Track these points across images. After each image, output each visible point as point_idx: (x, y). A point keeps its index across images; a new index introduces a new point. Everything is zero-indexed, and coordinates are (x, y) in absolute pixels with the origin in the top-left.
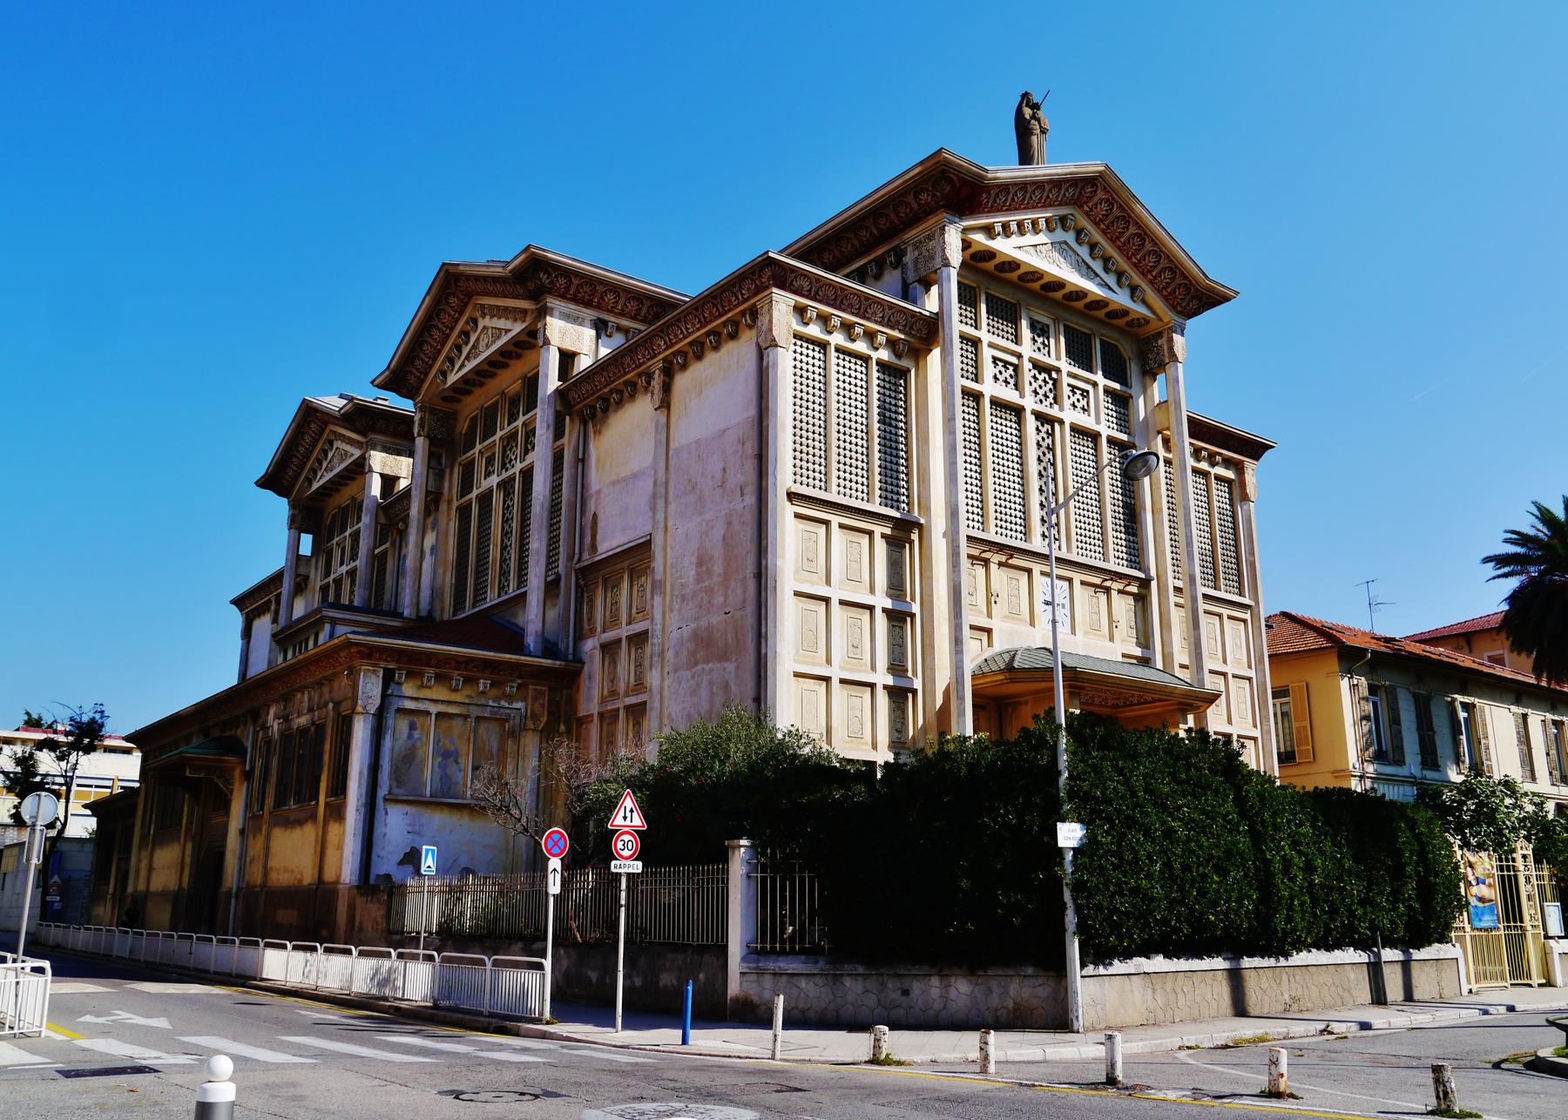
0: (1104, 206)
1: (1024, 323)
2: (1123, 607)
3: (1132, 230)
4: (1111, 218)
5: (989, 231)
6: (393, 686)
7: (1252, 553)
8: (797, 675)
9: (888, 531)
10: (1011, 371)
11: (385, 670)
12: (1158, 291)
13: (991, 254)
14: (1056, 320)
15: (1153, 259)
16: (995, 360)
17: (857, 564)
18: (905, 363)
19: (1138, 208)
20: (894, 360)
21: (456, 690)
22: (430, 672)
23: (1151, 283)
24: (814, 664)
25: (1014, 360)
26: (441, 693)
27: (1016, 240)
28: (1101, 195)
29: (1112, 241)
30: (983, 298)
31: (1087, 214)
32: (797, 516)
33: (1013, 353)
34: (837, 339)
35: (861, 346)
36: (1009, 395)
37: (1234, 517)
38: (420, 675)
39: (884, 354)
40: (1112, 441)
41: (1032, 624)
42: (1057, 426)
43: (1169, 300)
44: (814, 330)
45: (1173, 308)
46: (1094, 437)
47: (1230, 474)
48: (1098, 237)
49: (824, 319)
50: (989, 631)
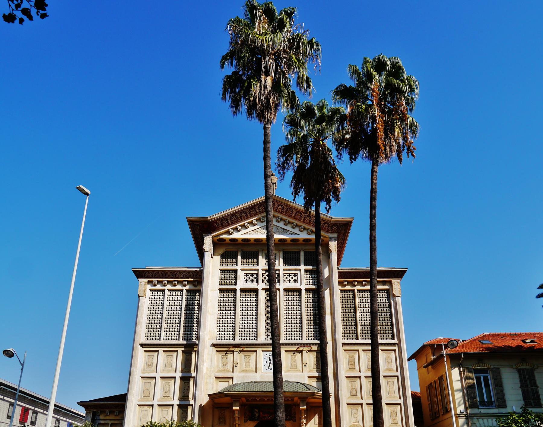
1: (260, 257)
2: (310, 358)
3: (295, 211)
5: (228, 233)
6: (97, 417)
7: (397, 319)
8: (139, 405)
9: (183, 349)
10: (255, 276)
11: (93, 412)
13: (234, 240)
14: (279, 251)
16: (246, 275)
18: (198, 288)
21: (116, 415)
22: (107, 411)
24: (149, 401)
25: (256, 272)
26: (112, 417)
27: (243, 231)
29: (291, 216)
30: (240, 254)
32: (145, 351)
33: (255, 270)
34: (169, 287)
35: (179, 287)
36: (253, 286)
38: (104, 412)
39: (187, 287)
40: (307, 290)
41: (256, 372)
44: (159, 287)
46: (299, 291)
47: (386, 287)
48: (284, 217)
50: (232, 378)
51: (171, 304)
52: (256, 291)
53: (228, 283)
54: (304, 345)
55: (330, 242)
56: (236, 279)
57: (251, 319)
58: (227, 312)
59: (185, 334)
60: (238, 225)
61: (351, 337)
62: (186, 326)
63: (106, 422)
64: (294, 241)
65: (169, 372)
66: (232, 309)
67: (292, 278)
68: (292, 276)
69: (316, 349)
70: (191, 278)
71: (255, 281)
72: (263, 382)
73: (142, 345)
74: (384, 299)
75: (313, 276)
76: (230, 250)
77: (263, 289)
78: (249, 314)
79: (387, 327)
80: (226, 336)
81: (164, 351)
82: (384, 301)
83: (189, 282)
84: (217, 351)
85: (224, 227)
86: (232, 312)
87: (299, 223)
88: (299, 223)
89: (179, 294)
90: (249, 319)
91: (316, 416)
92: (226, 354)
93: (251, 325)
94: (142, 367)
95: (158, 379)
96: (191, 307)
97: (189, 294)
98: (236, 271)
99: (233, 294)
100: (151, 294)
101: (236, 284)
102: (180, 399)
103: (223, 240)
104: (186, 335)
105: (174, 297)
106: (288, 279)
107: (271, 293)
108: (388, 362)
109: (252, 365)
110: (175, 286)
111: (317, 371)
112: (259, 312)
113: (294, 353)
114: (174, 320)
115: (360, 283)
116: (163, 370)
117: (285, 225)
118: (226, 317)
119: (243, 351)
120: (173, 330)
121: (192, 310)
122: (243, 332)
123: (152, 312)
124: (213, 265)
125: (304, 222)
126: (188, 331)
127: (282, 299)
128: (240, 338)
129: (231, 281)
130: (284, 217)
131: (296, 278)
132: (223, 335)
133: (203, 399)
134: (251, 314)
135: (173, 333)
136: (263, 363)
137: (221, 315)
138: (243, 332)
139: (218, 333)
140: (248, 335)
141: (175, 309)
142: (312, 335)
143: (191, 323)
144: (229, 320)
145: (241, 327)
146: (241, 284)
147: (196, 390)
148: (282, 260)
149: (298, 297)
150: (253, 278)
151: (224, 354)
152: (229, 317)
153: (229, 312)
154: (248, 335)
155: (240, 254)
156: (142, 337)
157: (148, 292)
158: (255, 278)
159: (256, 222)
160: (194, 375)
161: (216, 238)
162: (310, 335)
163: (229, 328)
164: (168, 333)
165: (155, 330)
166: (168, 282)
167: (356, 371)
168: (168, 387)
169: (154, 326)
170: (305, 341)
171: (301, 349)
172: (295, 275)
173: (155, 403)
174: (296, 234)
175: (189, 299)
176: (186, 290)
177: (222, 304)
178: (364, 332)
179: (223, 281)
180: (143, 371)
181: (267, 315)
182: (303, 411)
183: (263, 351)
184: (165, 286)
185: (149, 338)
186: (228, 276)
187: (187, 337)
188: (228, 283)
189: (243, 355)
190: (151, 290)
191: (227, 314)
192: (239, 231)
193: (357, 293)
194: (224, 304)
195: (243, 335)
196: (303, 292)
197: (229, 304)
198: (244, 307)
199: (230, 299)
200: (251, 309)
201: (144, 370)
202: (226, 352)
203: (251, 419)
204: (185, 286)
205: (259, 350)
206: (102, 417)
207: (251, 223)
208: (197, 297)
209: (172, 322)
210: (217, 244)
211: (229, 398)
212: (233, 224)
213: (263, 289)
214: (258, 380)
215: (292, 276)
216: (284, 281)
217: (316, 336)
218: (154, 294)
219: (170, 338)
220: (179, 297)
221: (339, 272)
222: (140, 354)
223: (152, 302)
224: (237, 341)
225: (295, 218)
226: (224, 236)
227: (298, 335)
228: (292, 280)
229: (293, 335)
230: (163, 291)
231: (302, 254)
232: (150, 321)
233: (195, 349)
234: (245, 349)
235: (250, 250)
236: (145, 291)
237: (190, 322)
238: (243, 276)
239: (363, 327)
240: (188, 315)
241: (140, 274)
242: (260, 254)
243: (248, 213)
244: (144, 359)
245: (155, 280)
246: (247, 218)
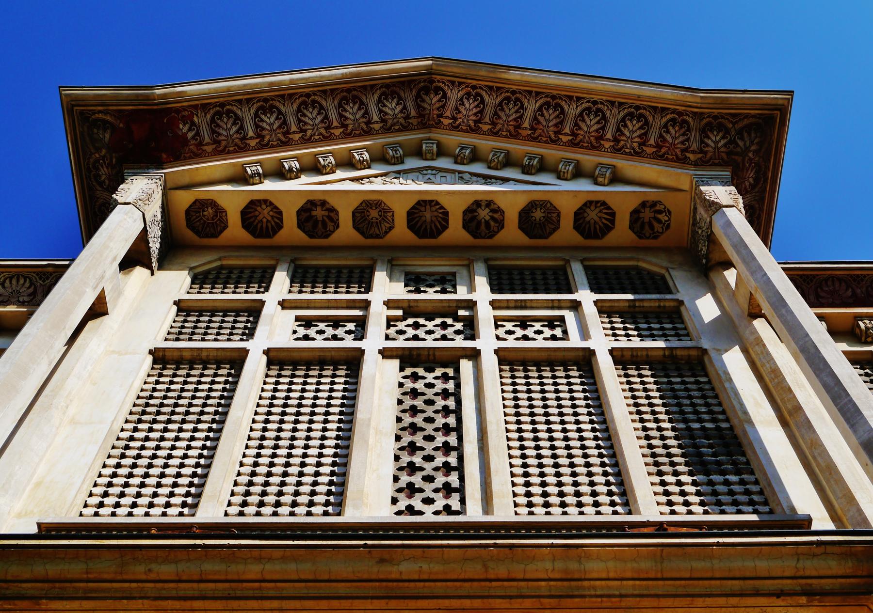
0: (470, 105)
3: (531, 106)
4: (489, 112)
12: (637, 154)
19: (514, 75)
23: (617, 150)
28: (454, 95)
31: (455, 128)
42: (466, 366)
43: (660, 156)
45: (681, 161)
77: (385, 353)
196: (605, 364)
243: (333, 115)
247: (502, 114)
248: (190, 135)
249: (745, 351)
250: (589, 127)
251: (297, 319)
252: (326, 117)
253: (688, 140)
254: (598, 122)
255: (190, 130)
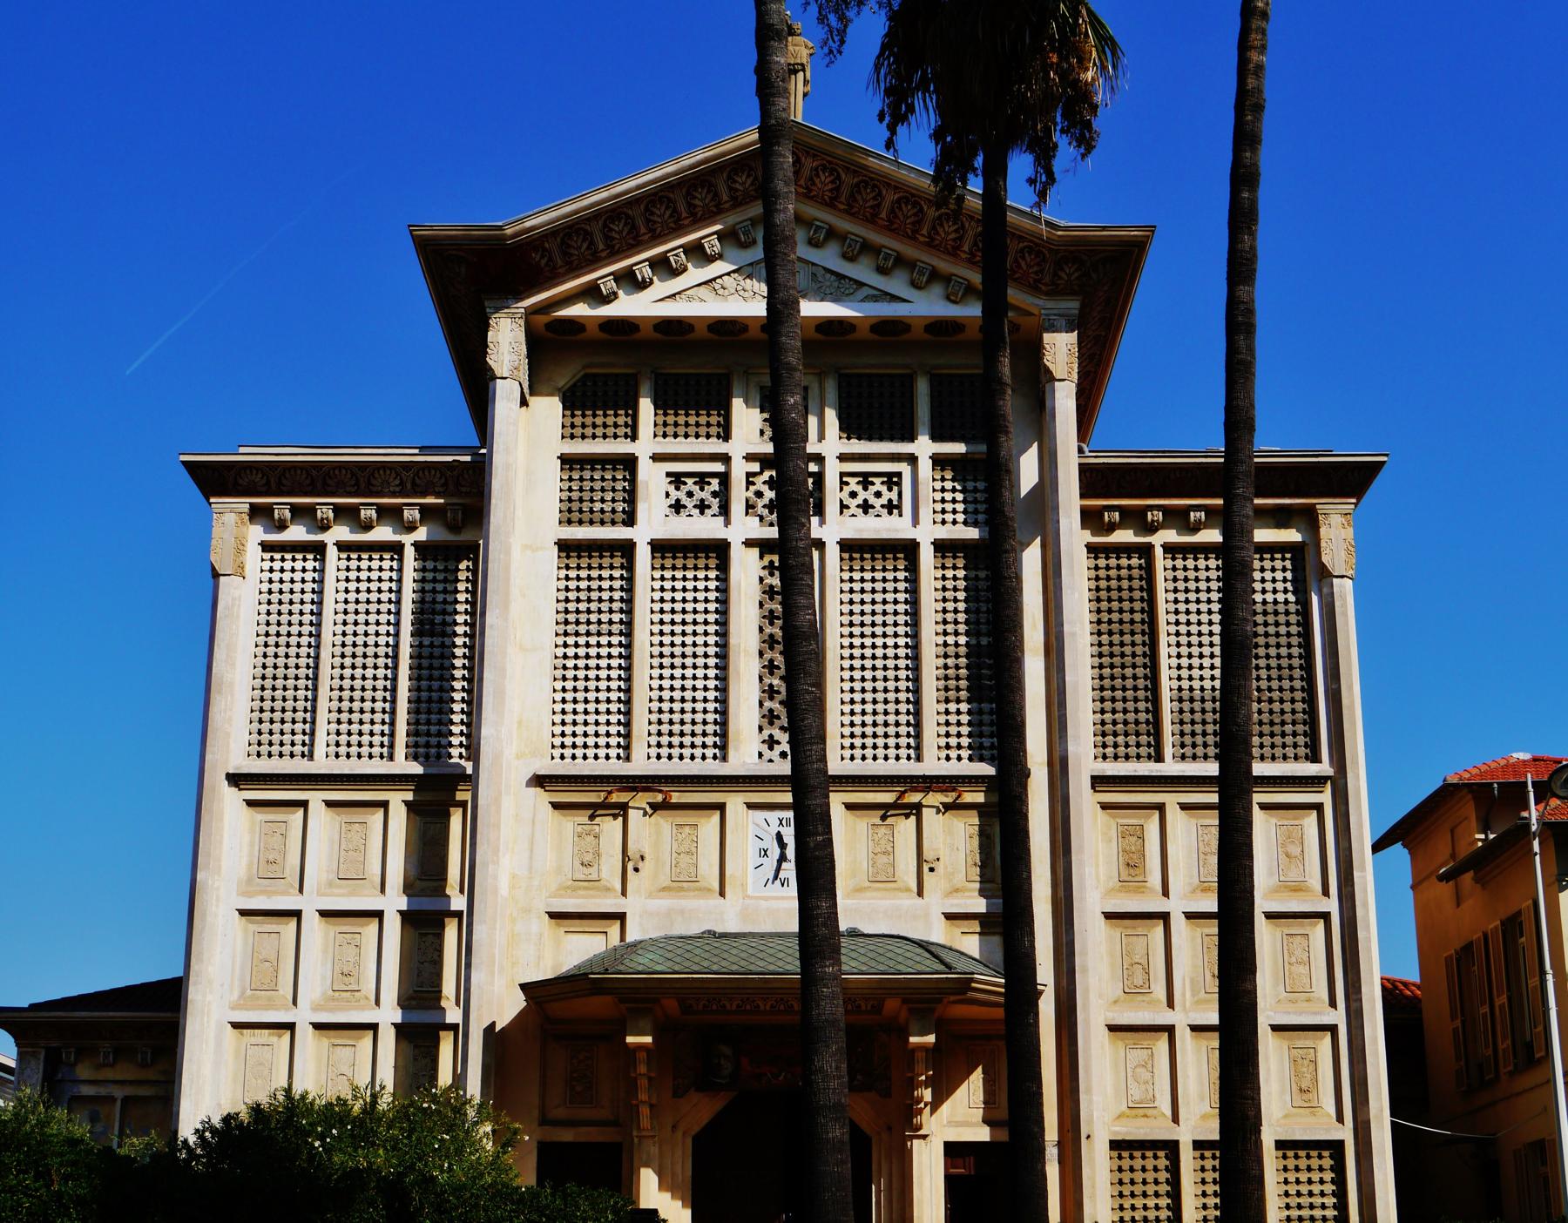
1: (738, 404)
2: (954, 839)
5: (593, 294)
8: (236, 1026)
9: (409, 796)
10: (715, 484)
11: (48, 1050)
15: (950, 227)
16: (677, 479)
17: (358, 856)
20: (451, 537)
25: (718, 467)
27: (661, 288)
29: (871, 220)
30: (645, 387)
32: (251, 803)
34: (342, 532)
35: (383, 533)
37: (1305, 613)
39: (421, 534)
40: (941, 547)
41: (722, 894)
46: (909, 549)
47: (1292, 535)
48: (843, 224)
49: (299, 513)
50: (621, 917)
51: (351, 607)
52: (718, 551)
53: (597, 517)
54: (929, 783)
55: (1047, 337)
56: (631, 497)
57: (700, 673)
58: (593, 640)
59: (417, 734)
60: (638, 261)
61: (1132, 751)
62: (418, 701)
63: (103, 1091)
64: (888, 329)
65: (352, 894)
66: (616, 628)
67: (878, 495)
68: (878, 484)
69: (979, 798)
70: (438, 496)
71: (715, 509)
72: (753, 935)
73: (237, 780)
74: (1280, 586)
75: (970, 485)
76: (600, 373)
77: (749, 543)
78: (689, 650)
79: (1287, 707)
80: (591, 741)
81: (330, 804)
82: (1281, 597)
83: (424, 510)
84: (556, 806)
85: (575, 270)
86: (615, 640)
87: (909, 251)
88: (909, 251)
89: (386, 564)
90: (689, 673)
91: (980, 1069)
92: (592, 817)
93: (700, 695)
94: (242, 872)
95: (311, 921)
96: (438, 619)
97: (430, 564)
98: (629, 463)
99: (617, 562)
100: (266, 565)
101: (630, 520)
102: (405, 1002)
103: (575, 324)
104: (422, 740)
105: (364, 575)
106: (859, 500)
107: (790, 558)
108: (1289, 855)
109: (703, 865)
110: (368, 527)
111: (983, 893)
112: (733, 640)
113: (884, 818)
114: (369, 673)
115: (1175, 517)
116: (330, 884)
117: (848, 257)
118: (592, 663)
119: (665, 806)
120: (367, 717)
121: (444, 634)
122: (665, 728)
123: (272, 640)
124: (530, 439)
125: (931, 245)
126: (428, 723)
127: (834, 588)
128: (654, 751)
129: (607, 507)
130: (843, 224)
131: (894, 496)
132: (580, 741)
133: (498, 1002)
134: (700, 650)
135: (366, 728)
136: (753, 858)
137: (571, 652)
138: (665, 728)
139: (558, 730)
140: (687, 740)
141: (372, 629)
142: (965, 741)
143: (441, 689)
144: (603, 674)
145: (655, 705)
146: (655, 520)
147: (468, 965)
148: (831, 416)
149: (901, 575)
150: (703, 495)
151: (582, 817)
152: (603, 663)
153: (604, 640)
154: (687, 740)
155: (645, 387)
156: (233, 743)
157: (254, 557)
158: (715, 494)
159: (717, 248)
160: (458, 903)
161: (542, 319)
162: (953, 741)
163: (603, 707)
164: (344, 728)
165: (288, 715)
166: (338, 509)
167: (1152, 890)
168: (352, 951)
169: (286, 697)
170: (933, 765)
171: (914, 798)
172: (892, 480)
173: (303, 1016)
174: (894, 298)
175: (428, 587)
176: (416, 545)
177: (572, 606)
178: (1187, 728)
179: (575, 506)
180: (246, 889)
181: (768, 656)
182: (920, 1055)
183: (750, 806)
184: (325, 528)
185: (264, 749)
186: (598, 485)
187: (427, 745)
188: (597, 517)
189: (664, 823)
190: (266, 547)
191: (593, 651)
192: (643, 285)
193: (1160, 561)
194: (583, 606)
195: (665, 740)
196: (927, 555)
197: (605, 606)
198: (667, 618)
199: (606, 584)
200: (700, 629)
201: (249, 881)
202: (594, 810)
203: (705, 1083)
204: (411, 528)
205: (735, 802)
206: (83, 1072)
207: (697, 253)
208: (462, 576)
209: (358, 683)
210: (549, 345)
211: (608, 999)
212: (615, 254)
213: (749, 543)
214: (732, 927)
215: (878, 484)
216: (843, 507)
217: (981, 747)
218: (277, 565)
219: (354, 750)
220: (386, 575)
221: (1084, 470)
222: (232, 822)
223: (272, 598)
224: (641, 763)
225: (891, 228)
226: (579, 310)
227: (903, 741)
228: (877, 503)
229: (880, 742)
230: (319, 549)
231: (922, 388)
232: (267, 681)
233: (460, 796)
234: (676, 798)
235: (695, 370)
236: (240, 549)
237: (435, 685)
238: (664, 484)
239: (1186, 706)
240: (426, 651)
241: (216, 480)
242: (735, 391)
243: (682, 207)
244: (246, 839)
245: (282, 504)
246: (679, 230)
247: (859, 197)
248: (543, 262)
249: (1044, 546)
250: (947, 234)
251: (668, 474)
252: (675, 210)
253: (1041, 271)
254: (956, 231)
255: (542, 257)
